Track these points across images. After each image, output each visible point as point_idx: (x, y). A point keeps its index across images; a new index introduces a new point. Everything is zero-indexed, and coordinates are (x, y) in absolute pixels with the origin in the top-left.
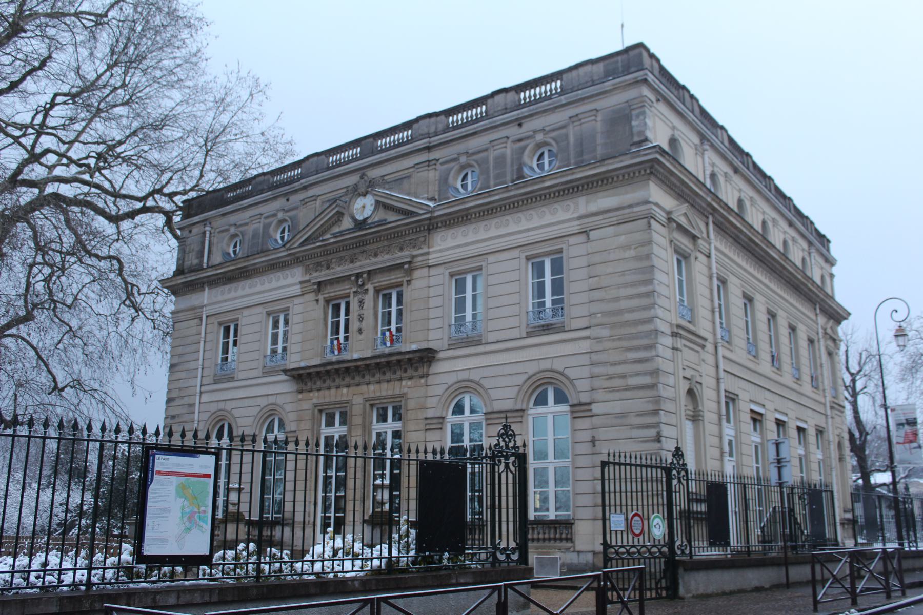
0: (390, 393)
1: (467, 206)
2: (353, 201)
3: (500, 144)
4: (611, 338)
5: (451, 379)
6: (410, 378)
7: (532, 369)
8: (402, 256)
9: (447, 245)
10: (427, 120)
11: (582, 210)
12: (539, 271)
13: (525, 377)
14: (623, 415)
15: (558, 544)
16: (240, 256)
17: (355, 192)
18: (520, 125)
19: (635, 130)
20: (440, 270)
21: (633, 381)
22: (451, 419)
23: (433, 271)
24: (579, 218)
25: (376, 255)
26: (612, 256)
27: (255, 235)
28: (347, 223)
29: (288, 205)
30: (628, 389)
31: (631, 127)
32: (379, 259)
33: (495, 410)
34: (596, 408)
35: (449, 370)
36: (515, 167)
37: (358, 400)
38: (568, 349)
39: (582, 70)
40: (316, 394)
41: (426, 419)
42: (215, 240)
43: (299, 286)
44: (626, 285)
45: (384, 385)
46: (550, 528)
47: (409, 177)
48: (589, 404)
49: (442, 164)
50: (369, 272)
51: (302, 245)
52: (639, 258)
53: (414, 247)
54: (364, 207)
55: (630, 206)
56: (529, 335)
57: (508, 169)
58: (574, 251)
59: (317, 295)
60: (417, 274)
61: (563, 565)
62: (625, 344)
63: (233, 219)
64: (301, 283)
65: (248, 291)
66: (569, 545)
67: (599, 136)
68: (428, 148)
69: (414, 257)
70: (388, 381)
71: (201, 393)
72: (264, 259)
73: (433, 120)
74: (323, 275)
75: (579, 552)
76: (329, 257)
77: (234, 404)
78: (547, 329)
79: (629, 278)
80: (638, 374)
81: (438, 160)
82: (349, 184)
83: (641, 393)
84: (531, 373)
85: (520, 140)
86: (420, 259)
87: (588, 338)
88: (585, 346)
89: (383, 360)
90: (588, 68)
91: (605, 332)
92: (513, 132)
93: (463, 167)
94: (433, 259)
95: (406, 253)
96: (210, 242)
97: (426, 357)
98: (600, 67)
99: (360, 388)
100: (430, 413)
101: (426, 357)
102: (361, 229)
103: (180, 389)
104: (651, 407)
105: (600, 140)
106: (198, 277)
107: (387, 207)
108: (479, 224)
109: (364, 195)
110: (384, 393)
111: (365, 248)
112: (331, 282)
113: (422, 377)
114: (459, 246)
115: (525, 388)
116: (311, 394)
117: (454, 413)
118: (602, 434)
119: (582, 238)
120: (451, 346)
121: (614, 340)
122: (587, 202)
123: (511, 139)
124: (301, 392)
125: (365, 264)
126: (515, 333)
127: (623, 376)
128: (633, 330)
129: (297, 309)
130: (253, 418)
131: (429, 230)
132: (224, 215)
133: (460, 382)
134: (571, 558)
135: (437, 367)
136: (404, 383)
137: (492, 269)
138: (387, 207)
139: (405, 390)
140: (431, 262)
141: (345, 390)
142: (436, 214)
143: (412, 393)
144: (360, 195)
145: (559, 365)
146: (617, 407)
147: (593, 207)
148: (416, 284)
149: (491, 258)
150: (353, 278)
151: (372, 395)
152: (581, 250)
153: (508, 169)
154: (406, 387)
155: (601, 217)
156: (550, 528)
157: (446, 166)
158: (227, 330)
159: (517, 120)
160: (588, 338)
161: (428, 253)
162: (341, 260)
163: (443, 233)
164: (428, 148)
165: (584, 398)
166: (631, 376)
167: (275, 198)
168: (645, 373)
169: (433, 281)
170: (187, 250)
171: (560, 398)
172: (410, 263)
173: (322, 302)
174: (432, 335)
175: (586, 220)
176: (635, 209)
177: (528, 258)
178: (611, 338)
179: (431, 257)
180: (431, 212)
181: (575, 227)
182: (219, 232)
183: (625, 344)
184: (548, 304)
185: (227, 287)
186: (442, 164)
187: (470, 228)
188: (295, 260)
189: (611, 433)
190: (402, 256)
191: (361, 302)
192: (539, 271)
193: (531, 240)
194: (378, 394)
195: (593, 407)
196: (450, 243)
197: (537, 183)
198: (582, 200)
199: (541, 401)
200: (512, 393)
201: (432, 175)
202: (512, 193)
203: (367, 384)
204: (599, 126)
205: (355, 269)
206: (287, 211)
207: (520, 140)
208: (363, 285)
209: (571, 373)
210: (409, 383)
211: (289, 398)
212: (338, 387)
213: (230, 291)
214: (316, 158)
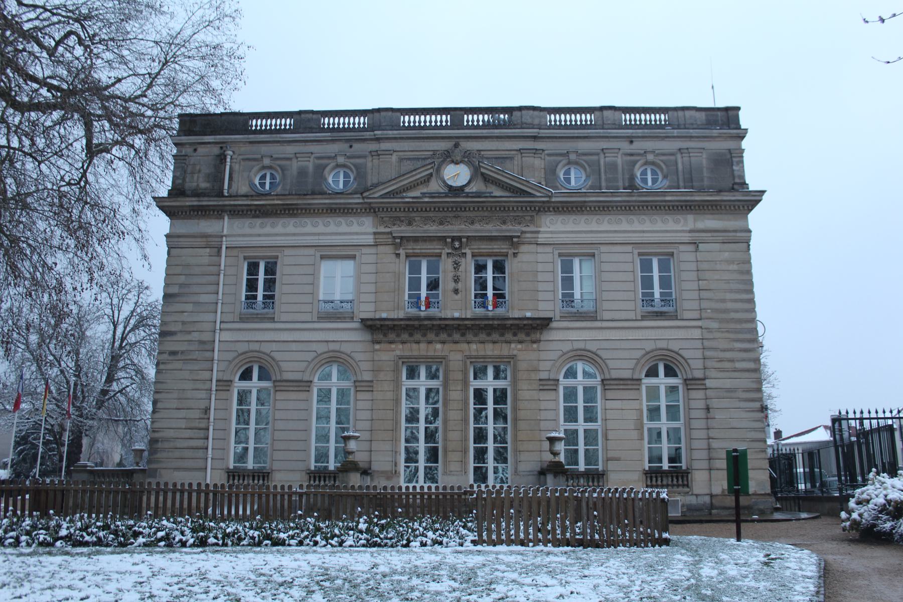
0: (496, 353)
1: (587, 199)
2: (444, 166)
3: (618, 152)
4: (719, 330)
5: (567, 347)
6: (520, 342)
7: (649, 346)
9: (554, 228)
10: (531, 112)
11: (690, 226)
12: (646, 267)
13: (643, 352)
14: (729, 390)
15: (680, 489)
16: (279, 189)
17: (448, 157)
18: (631, 142)
19: (736, 173)
20: (549, 249)
21: (739, 365)
22: (564, 382)
23: (540, 249)
24: (690, 231)
25: (472, 223)
26: (718, 267)
27: (302, 173)
28: (434, 186)
29: (350, 152)
30: (736, 370)
31: (733, 171)
32: (477, 226)
33: (614, 377)
34: (708, 383)
35: (563, 337)
36: (627, 176)
37: (459, 356)
38: (682, 334)
39: (687, 113)
40: (401, 346)
41: (540, 380)
42: (236, 167)
43: (372, 237)
44: (731, 291)
45: (489, 346)
46: (667, 477)
47: (512, 158)
48: (704, 379)
49: (549, 155)
50: (468, 238)
51: (381, 197)
52: (741, 272)
53: (520, 224)
54: (457, 174)
55: (735, 231)
56: (644, 318)
57: (620, 176)
58: (684, 257)
59: (396, 249)
60: (523, 248)
61: (683, 506)
62: (732, 336)
63: (264, 149)
64: (375, 233)
65: (291, 229)
66: (686, 489)
67: (705, 169)
68: (535, 138)
69: (523, 232)
70: (494, 342)
71: (220, 330)
72: (327, 201)
73: (536, 113)
75: (697, 495)
76: (414, 214)
77: (274, 347)
78: (660, 315)
79: (734, 286)
80: (743, 360)
81: (543, 150)
82: (436, 148)
83: (747, 375)
84: (648, 349)
85: (632, 155)
86: (528, 235)
87: (701, 327)
88: (697, 333)
89: (496, 322)
90: (693, 113)
91: (714, 325)
92: (625, 146)
93: (569, 163)
95: (518, 227)
96: (231, 167)
97: (543, 324)
99: (459, 345)
100: (544, 375)
101: (543, 324)
102: (456, 196)
103: (183, 323)
104: (754, 386)
105: (706, 174)
106: (220, 203)
107: (486, 179)
108: (592, 217)
109: (457, 163)
110: (489, 353)
111: (460, 214)
112: (416, 239)
113: (534, 342)
114: (592, 232)
115: (643, 361)
116: (393, 346)
117: (566, 376)
118: (714, 403)
119: (691, 248)
120: (563, 318)
121: (722, 332)
122: (695, 220)
123: (621, 152)
124: (375, 342)
126: (632, 315)
127: (732, 361)
128: (738, 326)
130: (305, 364)
131: (539, 210)
132: (251, 142)
133: (576, 350)
134: (692, 500)
135: (547, 335)
136: (513, 345)
137: (604, 257)
138: (486, 179)
139: (515, 352)
140: (540, 241)
141: (439, 346)
142: (553, 199)
143: (521, 356)
144: (452, 162)
145: (674, 346)
146: (728, 384)
147: (701, 225)
149: (603, 248)
150: (449, 240)
151: (474, 353)
152: (691, 257)
153: (620, 176)
155: (709, 234)
156: (667, 477)
157: (552, 158)
158: (253, 268)
159: (628, 137)
160: (701, 327)
161: (538, 232)
162: (426, 220)
163: (552, 217)
164: (535, 138)
165: (698, 374)
166: (738, 361)
167: (333, 141)
168: (750, 360)
169: (540, 258)
170: (189, 170)
171: (670, 372)
172: (518, 237)
173: (403, 256)
174: (542, 306)
175: (697, 234)
176: (738, 234)
177: (640, 254)
178: (719, 330)
179: (540, 236)
180: (550, 197)
181: (686, 237)
182: (244, 160)
183: (732, 336)
184: (657, 295)
185: (258, 221)
186: (549, 155)
187: (583, 218)
188: (370, 210)
189: (725, 403)
191: (457, 265)
192: (646, 267)
193: (645, 240)
194: (482, 353)
195: (707, 382)
196: (559, 227)
197: (658, 196)
198: (690, 217)
199: (652, 372)
201: (538, 163)
202: (634, 199)
203: (468, 343)
204: (704, 162)
205: (452, 231)
206: (349, 157)
207: (632, 155)
208: (461, 247)
209: (684, 353)
210: (519, 346)
211: (359, 347)
212: (430, 342)
213: (262, 226)
214: (390, 113)
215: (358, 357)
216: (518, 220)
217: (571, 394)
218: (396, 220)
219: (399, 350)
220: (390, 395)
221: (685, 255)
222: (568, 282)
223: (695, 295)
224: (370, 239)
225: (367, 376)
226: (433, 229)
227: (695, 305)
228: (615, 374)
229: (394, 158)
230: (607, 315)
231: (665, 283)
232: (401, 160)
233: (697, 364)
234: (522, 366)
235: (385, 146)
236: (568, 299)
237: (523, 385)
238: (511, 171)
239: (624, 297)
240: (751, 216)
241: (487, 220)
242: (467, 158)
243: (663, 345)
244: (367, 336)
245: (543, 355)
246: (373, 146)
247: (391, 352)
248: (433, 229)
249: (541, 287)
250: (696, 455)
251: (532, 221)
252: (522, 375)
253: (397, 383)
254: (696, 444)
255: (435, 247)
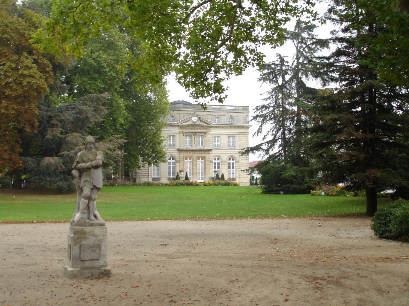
5: (215, 155)
7: (230, 155)
8: (205, 131)
9: (213, 131)
17: (193, 115)
35: (214, 153)
58: (237, 137)
60: (207, 135)
74: (184, 130)
78: (231, 149)
92: (227, 114)
94: (211, 133)
97: (211, 150)
98: (242, 108)
101: (211, 150)
125: (195, 130)
129: (177, 136)
135: (211, 152)
138: (201, 120)
143: (207, 156)
148: (207, 137)
154: (205, 155)
162: (189, 129)
169: (210, 137)
188: (178, 126)
189: (242, 166)
190: (205, 131)
198: (238, 129)
200: (226, 158)
211: (176, 154)
215: (176, 156)
216: (206, 129)
217: (215, 164)
218: (183, 128)
219: (184, 154)
220: (183, 163)
221: (237, 137)
222: (215, 141)
223: (238, 145)
224: (178, 132)
225: (178, 160)
226: (190, 130)
227: (238, 147)
228: (223, 160)
229: (182, 115)
230: (222, 149)
231: (233, 142)
232: (184, 115)
233: (238, 158)
234: (207, 158)
235: (181, 112)
236: (215, 146)
237: (207, 162)
238: (205, 118)
239: (225, 145)
240: (249, 129)
241: (200, 129)
242: (197, 116)
243: (232, 154)
244: (178, 152)
245: (210, 156)
246: (178, 112)
247: (183, 155)
248: (190, 130)
249: (210, 143)
250: (237, 175)
251: (209, 129)
252: (207, 160)
253: (184, 160)
254: (237, 173)
255: (191, 134)
